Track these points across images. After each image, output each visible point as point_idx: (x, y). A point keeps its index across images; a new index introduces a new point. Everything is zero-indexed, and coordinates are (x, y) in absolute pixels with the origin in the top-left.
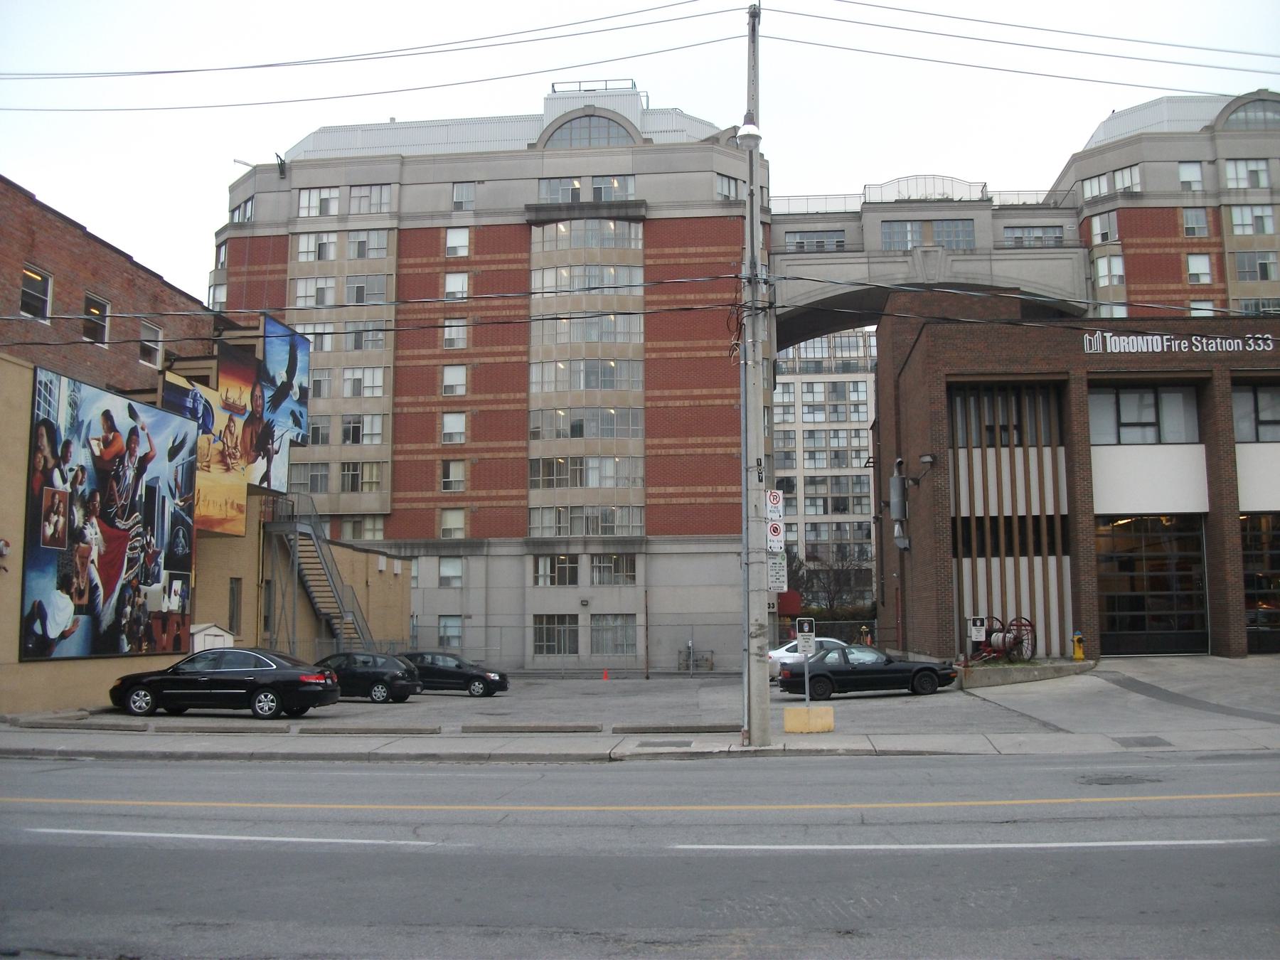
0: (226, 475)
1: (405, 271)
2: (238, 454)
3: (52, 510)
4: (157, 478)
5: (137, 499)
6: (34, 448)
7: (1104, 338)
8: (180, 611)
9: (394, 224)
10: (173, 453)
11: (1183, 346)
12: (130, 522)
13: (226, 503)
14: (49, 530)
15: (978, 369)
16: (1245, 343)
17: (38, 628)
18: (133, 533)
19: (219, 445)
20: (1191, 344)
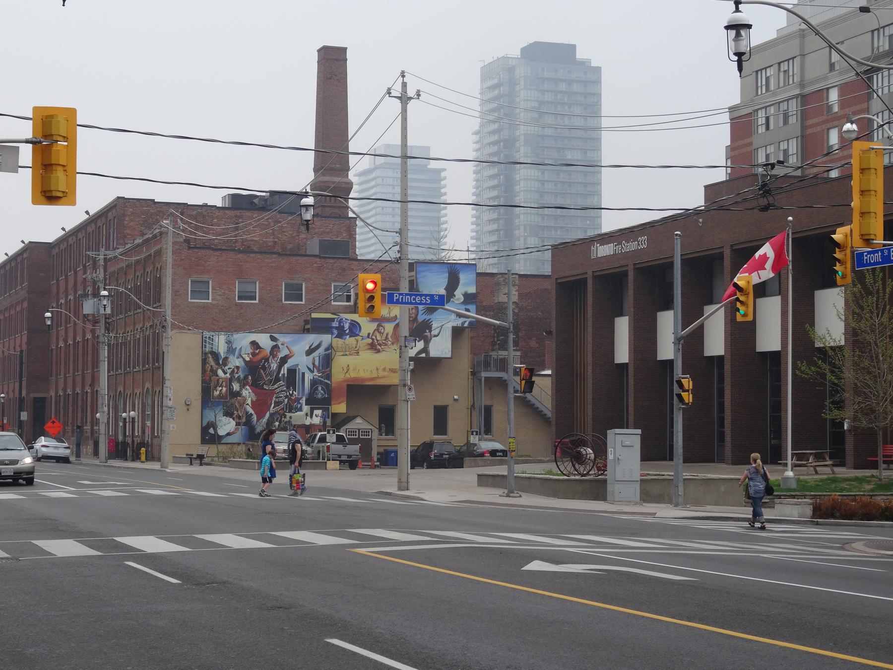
0: (377, 355)
1: (809, 131)
2: (390, 343)
3: (217, 384)
4: (297, 365)
5: (280, 375)
6: (204, 362)
7: (597, 247)
8: (322, 424)
9: (797, 91)
10: (309, 352)
11: (620, 249)
12: (276, 386)
13: (377, 369)
14: (216, 393)
15: (574, 273)
16: (639, 245)
17: (211, 431)
18: (278, 390)
19: (370, 341)
20: (622, 248)
